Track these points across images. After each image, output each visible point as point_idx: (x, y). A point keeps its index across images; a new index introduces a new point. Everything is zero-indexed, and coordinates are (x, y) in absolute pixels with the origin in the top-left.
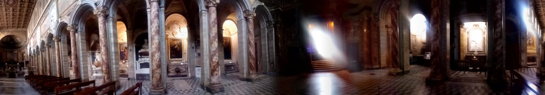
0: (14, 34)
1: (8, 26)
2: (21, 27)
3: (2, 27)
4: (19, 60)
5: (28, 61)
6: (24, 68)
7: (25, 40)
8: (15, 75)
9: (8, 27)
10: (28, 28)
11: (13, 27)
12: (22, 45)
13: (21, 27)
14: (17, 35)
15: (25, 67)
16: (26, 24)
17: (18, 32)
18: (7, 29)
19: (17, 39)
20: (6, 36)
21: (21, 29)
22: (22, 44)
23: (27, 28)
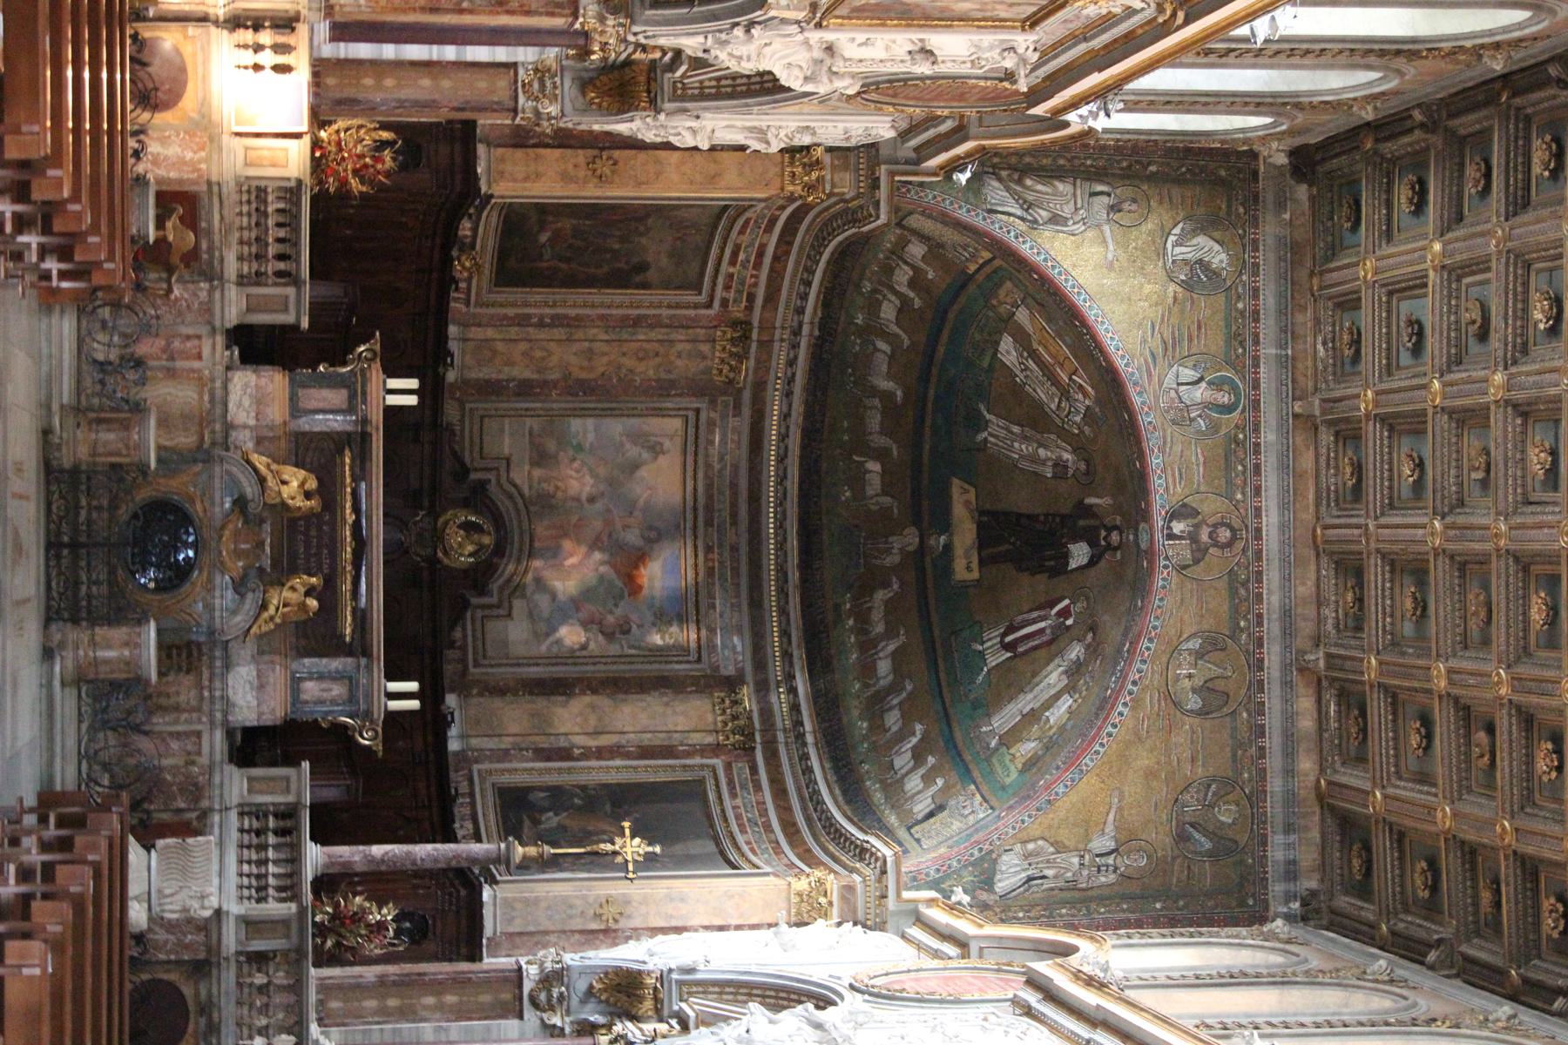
0: (1163, 578)
1: (1373, 434)
2: (1352, 778)
3: (1349, 303)
4: (514, 717)
5: (475, 956)
6: (288, 814)
7: (1010, 874)
8: (121, 612)
9: (1348, 434)
10: (1319, 949)
11: (1350, 568)
12: (894, 788)
13: (1352, 778)
14: (1143, 670)
15: (315, 856)
16: (1431, 908)
17: (1213, 697)
18: (1306, 422)
19: (1054, 677)
20: (1110, 381)
21: (1306, 764)
22: (920, 792)
23: (1312, 913)
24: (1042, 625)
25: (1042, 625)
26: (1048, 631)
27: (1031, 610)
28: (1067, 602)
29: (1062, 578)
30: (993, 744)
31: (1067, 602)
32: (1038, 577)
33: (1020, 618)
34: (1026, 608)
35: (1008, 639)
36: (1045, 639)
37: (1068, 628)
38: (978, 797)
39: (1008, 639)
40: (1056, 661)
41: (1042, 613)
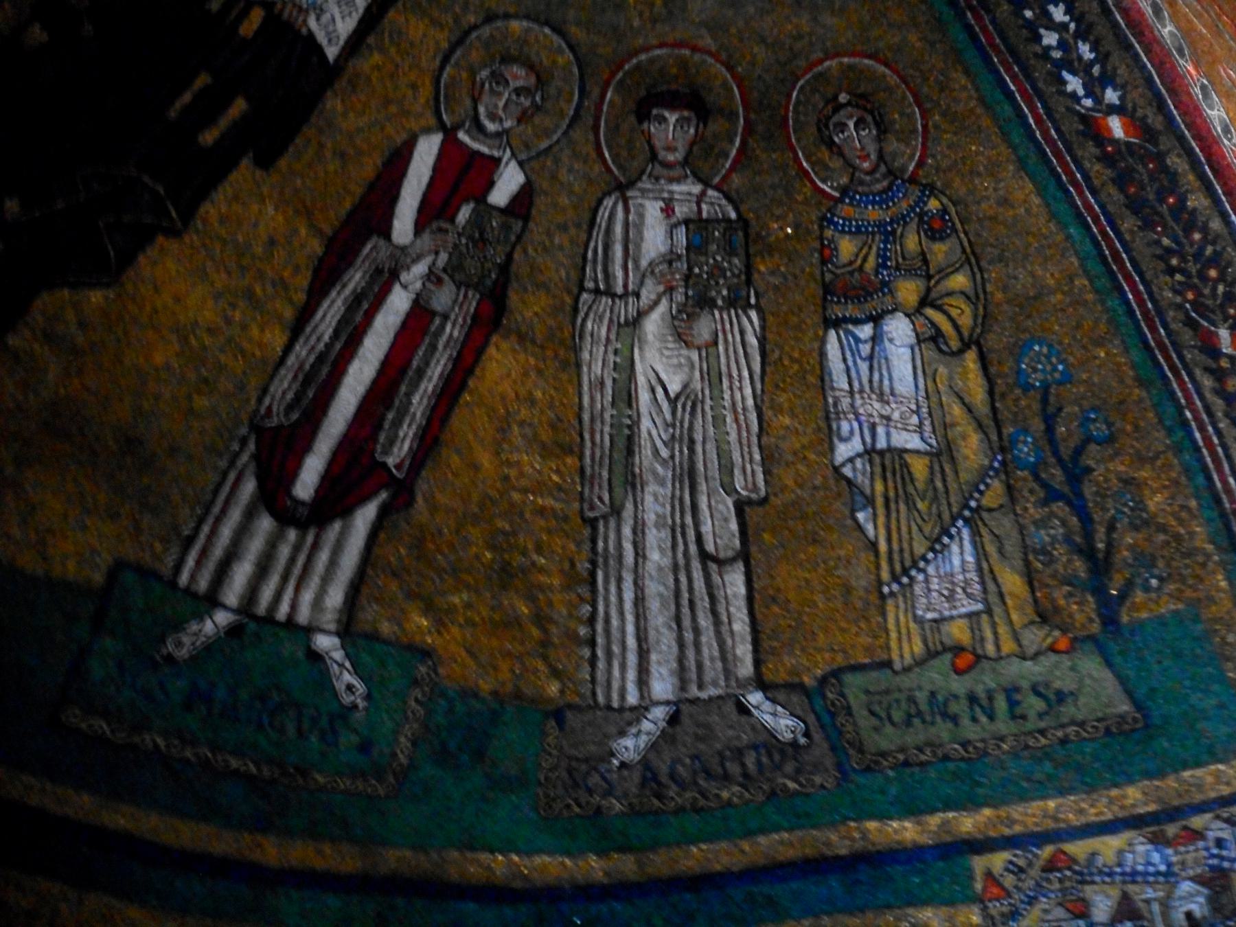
24: (399, 302)
25: (399, 302)
26: (443, 298)
27: (297, 329)
28: (427, 151)
29: (333, 103)
30: (783, 724)
31: (427, 151)
32: (213, 209)
33: (284, 386)
34: (276, 339)
35: (307, 482)
36: (453, 331)
37: (523, 201)
38: (1109, 846)
39: (307, 482)
40: (597, 327)
41: (355, 279)
